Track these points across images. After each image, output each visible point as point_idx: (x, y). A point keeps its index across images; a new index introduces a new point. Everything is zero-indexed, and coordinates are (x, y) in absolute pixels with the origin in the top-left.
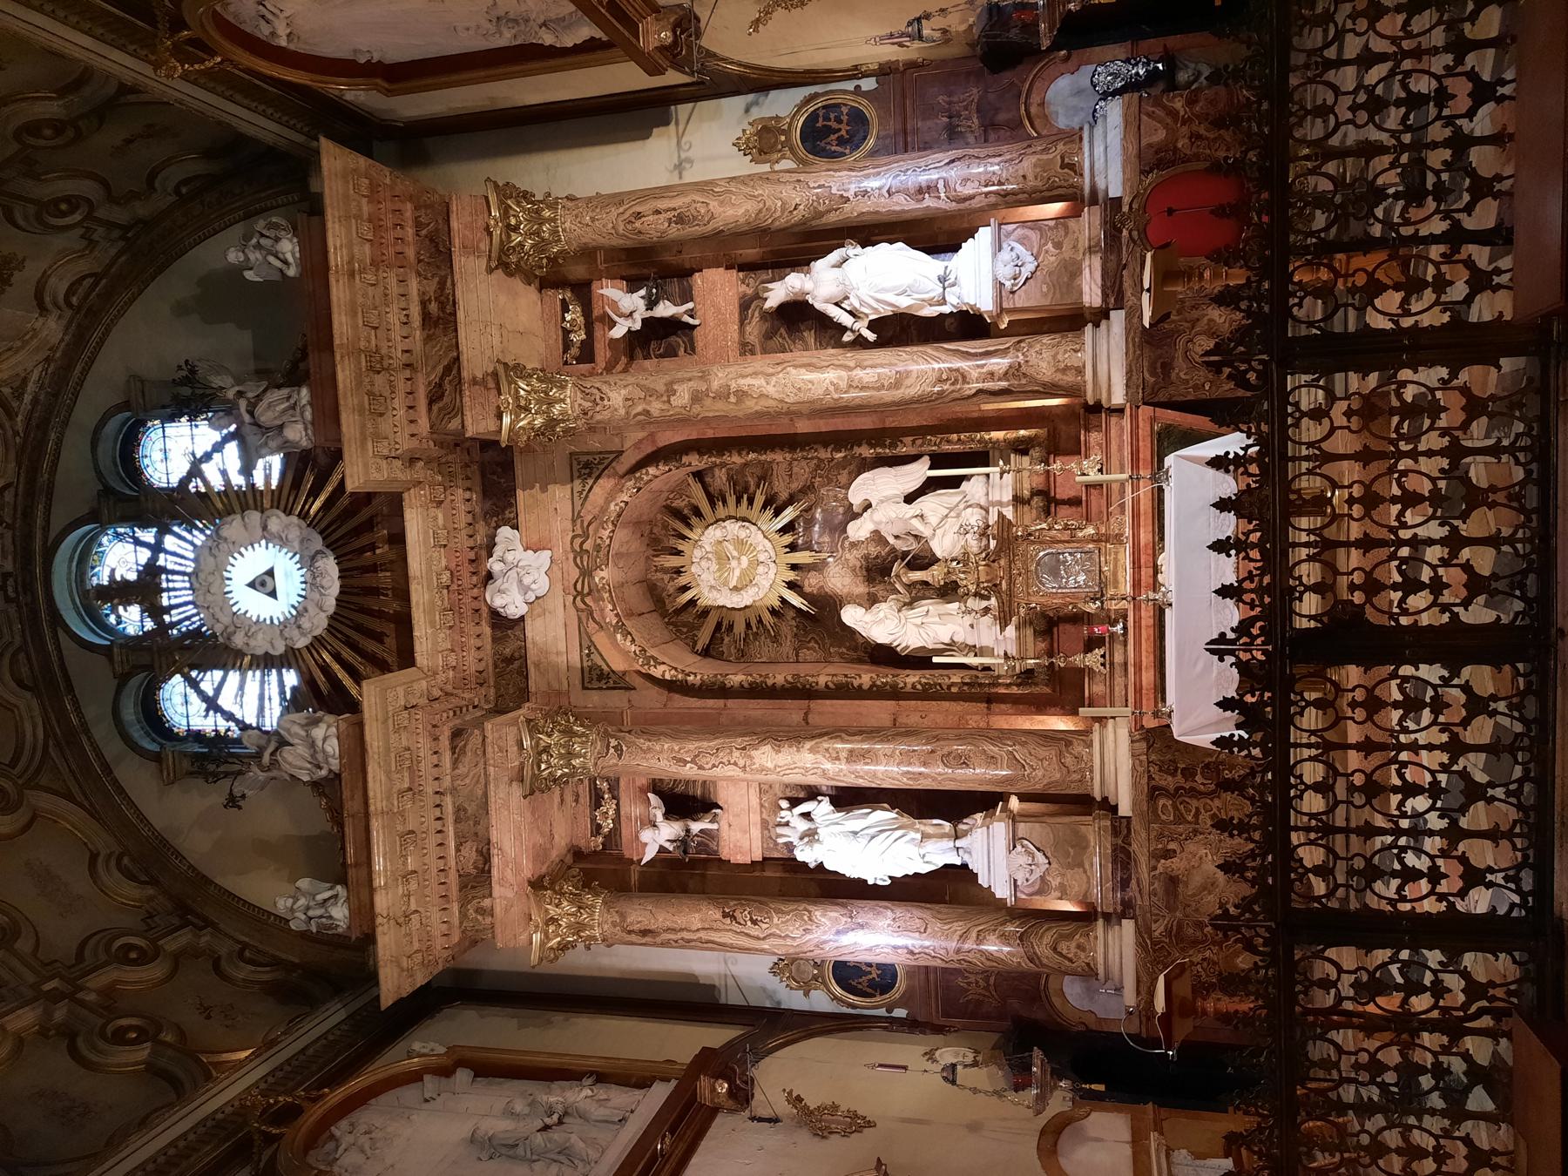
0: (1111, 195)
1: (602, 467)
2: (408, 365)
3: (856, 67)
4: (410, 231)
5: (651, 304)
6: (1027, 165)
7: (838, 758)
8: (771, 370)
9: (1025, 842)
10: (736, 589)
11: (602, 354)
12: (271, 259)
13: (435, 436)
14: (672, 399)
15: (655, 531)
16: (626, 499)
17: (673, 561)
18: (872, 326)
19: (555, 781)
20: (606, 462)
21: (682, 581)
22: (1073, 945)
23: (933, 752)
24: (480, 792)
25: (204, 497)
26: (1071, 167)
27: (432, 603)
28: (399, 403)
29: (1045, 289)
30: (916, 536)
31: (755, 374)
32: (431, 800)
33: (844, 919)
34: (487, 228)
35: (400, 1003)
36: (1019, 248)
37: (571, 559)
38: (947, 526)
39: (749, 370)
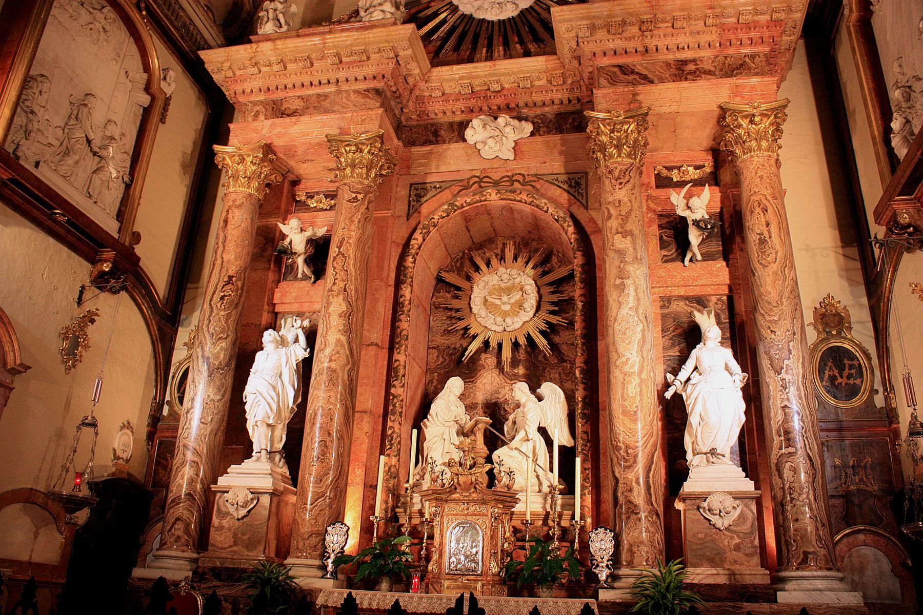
0: (778, 593)
2: (647, 50)
3: (892, 389)
4: (748, 50)
5: (696, 223)
8: (641, 312)
9: (255, 502)
10: (486, 301)
13: (596, 72)
14: (620, 235)
15: (535, 243)
16: (550, 211)
17: (509, 255)
18: (677, 397)
20: (580, 198)
21: (494, 261)
23: (329, 434)
24: (335, 109)
29: (700, 536)
32: (333, 77)
35: (202, 63)
36: (736, 514)
37: (507, 174)
39: (641, 295)
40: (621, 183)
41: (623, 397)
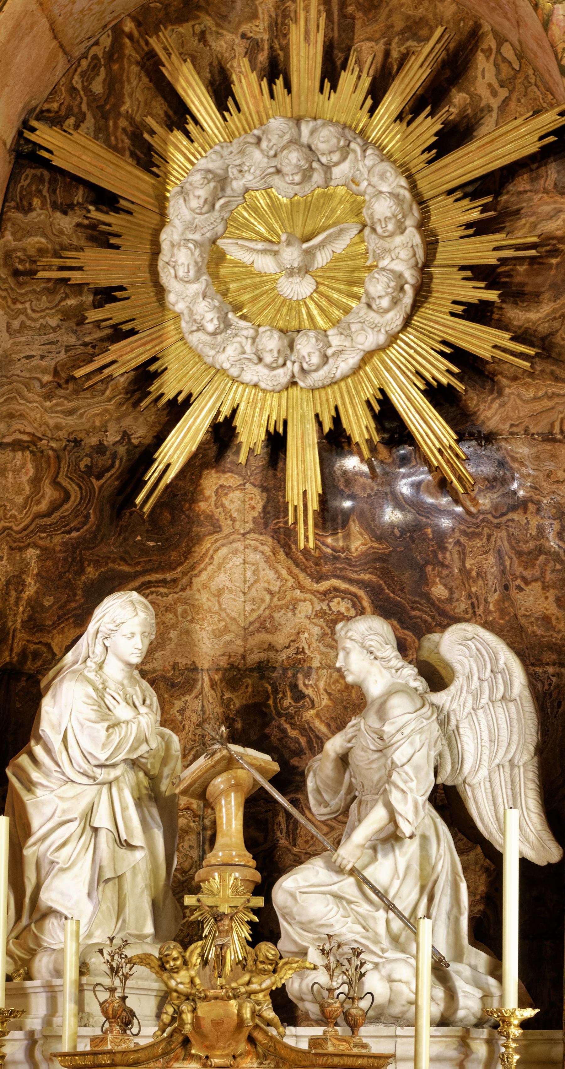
30: (346, 812)
38: (364, 908)
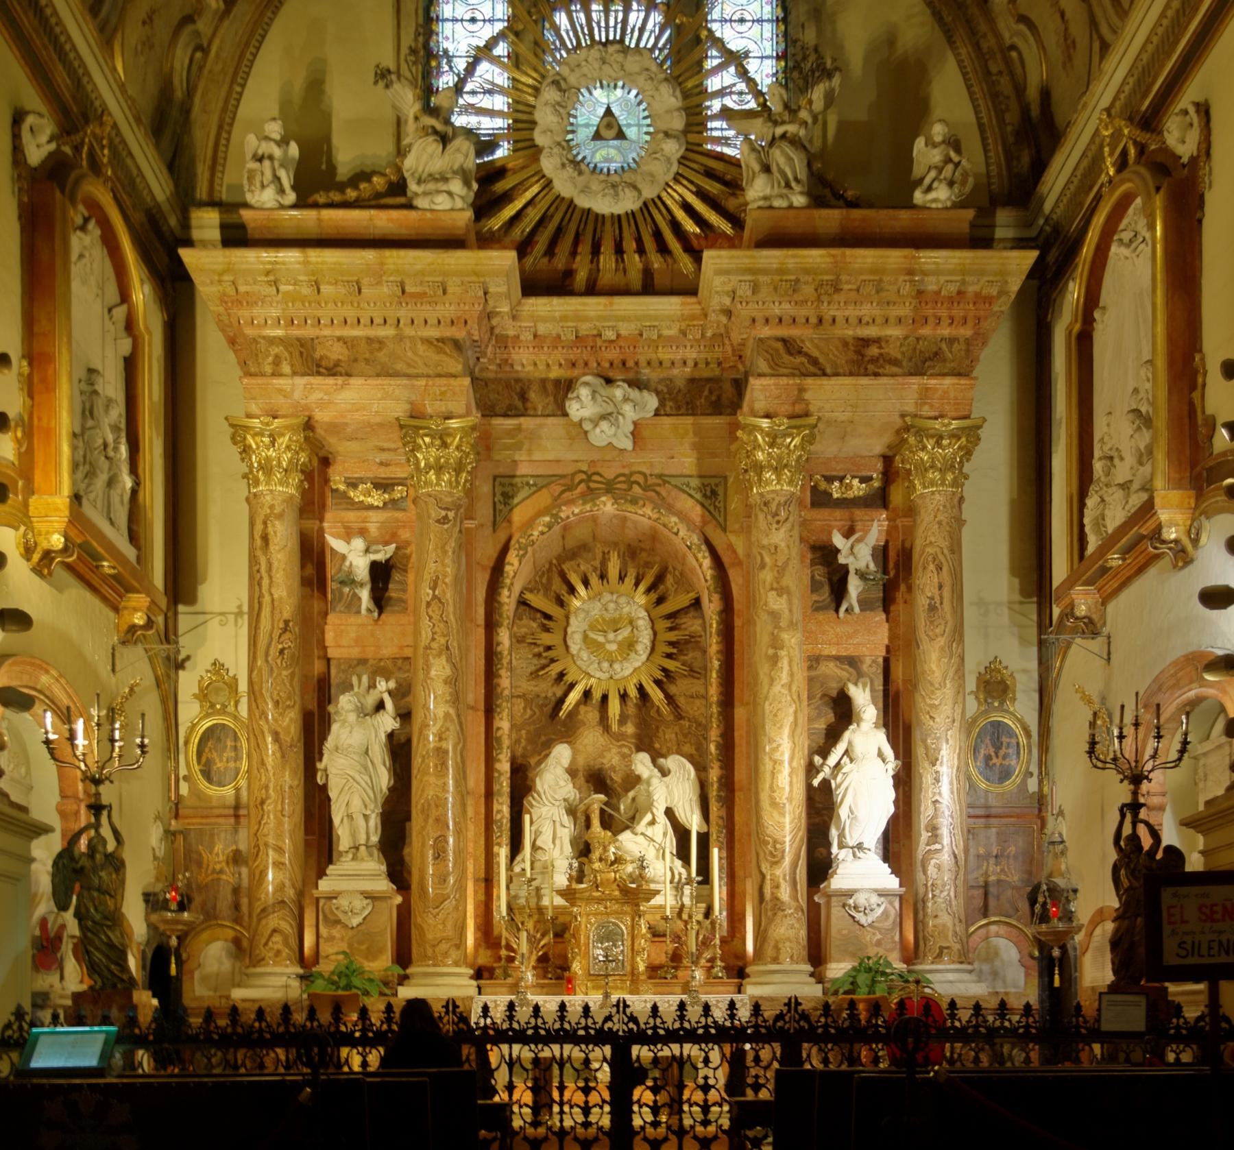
1: (712, 508)
5: (862, 575)
6: (945, 919)
7: (441, 739)
8: (794, 688)
9: (370, 908)
11: (821, 516)
12: (933, 174)
14: (774, 593)
19: (412, 451)
22: (280, 946)
25: (698, 67)
26: (940, 955)
27: (585, 319)
28: (785, 309)
29: (845, 932)
31: (792, 675)
33: (288, 739)
34: (942, 416)
36: (879, 911)
39: (795, 669)
40: (778, 522)
41: (771, 787)
